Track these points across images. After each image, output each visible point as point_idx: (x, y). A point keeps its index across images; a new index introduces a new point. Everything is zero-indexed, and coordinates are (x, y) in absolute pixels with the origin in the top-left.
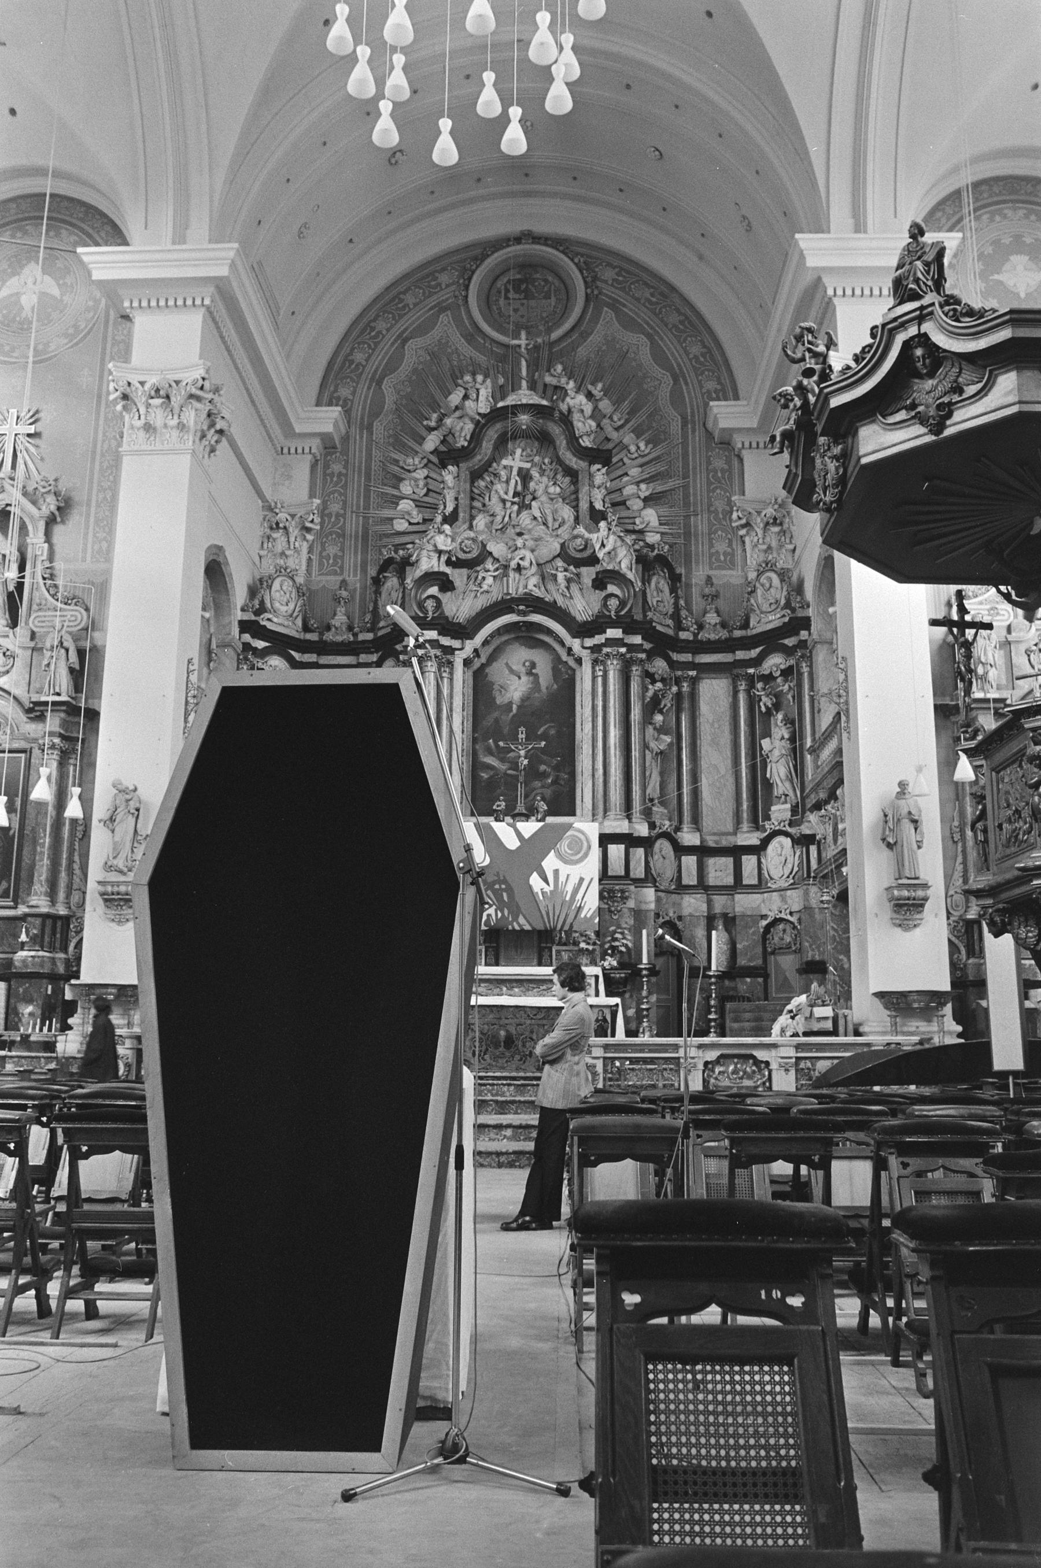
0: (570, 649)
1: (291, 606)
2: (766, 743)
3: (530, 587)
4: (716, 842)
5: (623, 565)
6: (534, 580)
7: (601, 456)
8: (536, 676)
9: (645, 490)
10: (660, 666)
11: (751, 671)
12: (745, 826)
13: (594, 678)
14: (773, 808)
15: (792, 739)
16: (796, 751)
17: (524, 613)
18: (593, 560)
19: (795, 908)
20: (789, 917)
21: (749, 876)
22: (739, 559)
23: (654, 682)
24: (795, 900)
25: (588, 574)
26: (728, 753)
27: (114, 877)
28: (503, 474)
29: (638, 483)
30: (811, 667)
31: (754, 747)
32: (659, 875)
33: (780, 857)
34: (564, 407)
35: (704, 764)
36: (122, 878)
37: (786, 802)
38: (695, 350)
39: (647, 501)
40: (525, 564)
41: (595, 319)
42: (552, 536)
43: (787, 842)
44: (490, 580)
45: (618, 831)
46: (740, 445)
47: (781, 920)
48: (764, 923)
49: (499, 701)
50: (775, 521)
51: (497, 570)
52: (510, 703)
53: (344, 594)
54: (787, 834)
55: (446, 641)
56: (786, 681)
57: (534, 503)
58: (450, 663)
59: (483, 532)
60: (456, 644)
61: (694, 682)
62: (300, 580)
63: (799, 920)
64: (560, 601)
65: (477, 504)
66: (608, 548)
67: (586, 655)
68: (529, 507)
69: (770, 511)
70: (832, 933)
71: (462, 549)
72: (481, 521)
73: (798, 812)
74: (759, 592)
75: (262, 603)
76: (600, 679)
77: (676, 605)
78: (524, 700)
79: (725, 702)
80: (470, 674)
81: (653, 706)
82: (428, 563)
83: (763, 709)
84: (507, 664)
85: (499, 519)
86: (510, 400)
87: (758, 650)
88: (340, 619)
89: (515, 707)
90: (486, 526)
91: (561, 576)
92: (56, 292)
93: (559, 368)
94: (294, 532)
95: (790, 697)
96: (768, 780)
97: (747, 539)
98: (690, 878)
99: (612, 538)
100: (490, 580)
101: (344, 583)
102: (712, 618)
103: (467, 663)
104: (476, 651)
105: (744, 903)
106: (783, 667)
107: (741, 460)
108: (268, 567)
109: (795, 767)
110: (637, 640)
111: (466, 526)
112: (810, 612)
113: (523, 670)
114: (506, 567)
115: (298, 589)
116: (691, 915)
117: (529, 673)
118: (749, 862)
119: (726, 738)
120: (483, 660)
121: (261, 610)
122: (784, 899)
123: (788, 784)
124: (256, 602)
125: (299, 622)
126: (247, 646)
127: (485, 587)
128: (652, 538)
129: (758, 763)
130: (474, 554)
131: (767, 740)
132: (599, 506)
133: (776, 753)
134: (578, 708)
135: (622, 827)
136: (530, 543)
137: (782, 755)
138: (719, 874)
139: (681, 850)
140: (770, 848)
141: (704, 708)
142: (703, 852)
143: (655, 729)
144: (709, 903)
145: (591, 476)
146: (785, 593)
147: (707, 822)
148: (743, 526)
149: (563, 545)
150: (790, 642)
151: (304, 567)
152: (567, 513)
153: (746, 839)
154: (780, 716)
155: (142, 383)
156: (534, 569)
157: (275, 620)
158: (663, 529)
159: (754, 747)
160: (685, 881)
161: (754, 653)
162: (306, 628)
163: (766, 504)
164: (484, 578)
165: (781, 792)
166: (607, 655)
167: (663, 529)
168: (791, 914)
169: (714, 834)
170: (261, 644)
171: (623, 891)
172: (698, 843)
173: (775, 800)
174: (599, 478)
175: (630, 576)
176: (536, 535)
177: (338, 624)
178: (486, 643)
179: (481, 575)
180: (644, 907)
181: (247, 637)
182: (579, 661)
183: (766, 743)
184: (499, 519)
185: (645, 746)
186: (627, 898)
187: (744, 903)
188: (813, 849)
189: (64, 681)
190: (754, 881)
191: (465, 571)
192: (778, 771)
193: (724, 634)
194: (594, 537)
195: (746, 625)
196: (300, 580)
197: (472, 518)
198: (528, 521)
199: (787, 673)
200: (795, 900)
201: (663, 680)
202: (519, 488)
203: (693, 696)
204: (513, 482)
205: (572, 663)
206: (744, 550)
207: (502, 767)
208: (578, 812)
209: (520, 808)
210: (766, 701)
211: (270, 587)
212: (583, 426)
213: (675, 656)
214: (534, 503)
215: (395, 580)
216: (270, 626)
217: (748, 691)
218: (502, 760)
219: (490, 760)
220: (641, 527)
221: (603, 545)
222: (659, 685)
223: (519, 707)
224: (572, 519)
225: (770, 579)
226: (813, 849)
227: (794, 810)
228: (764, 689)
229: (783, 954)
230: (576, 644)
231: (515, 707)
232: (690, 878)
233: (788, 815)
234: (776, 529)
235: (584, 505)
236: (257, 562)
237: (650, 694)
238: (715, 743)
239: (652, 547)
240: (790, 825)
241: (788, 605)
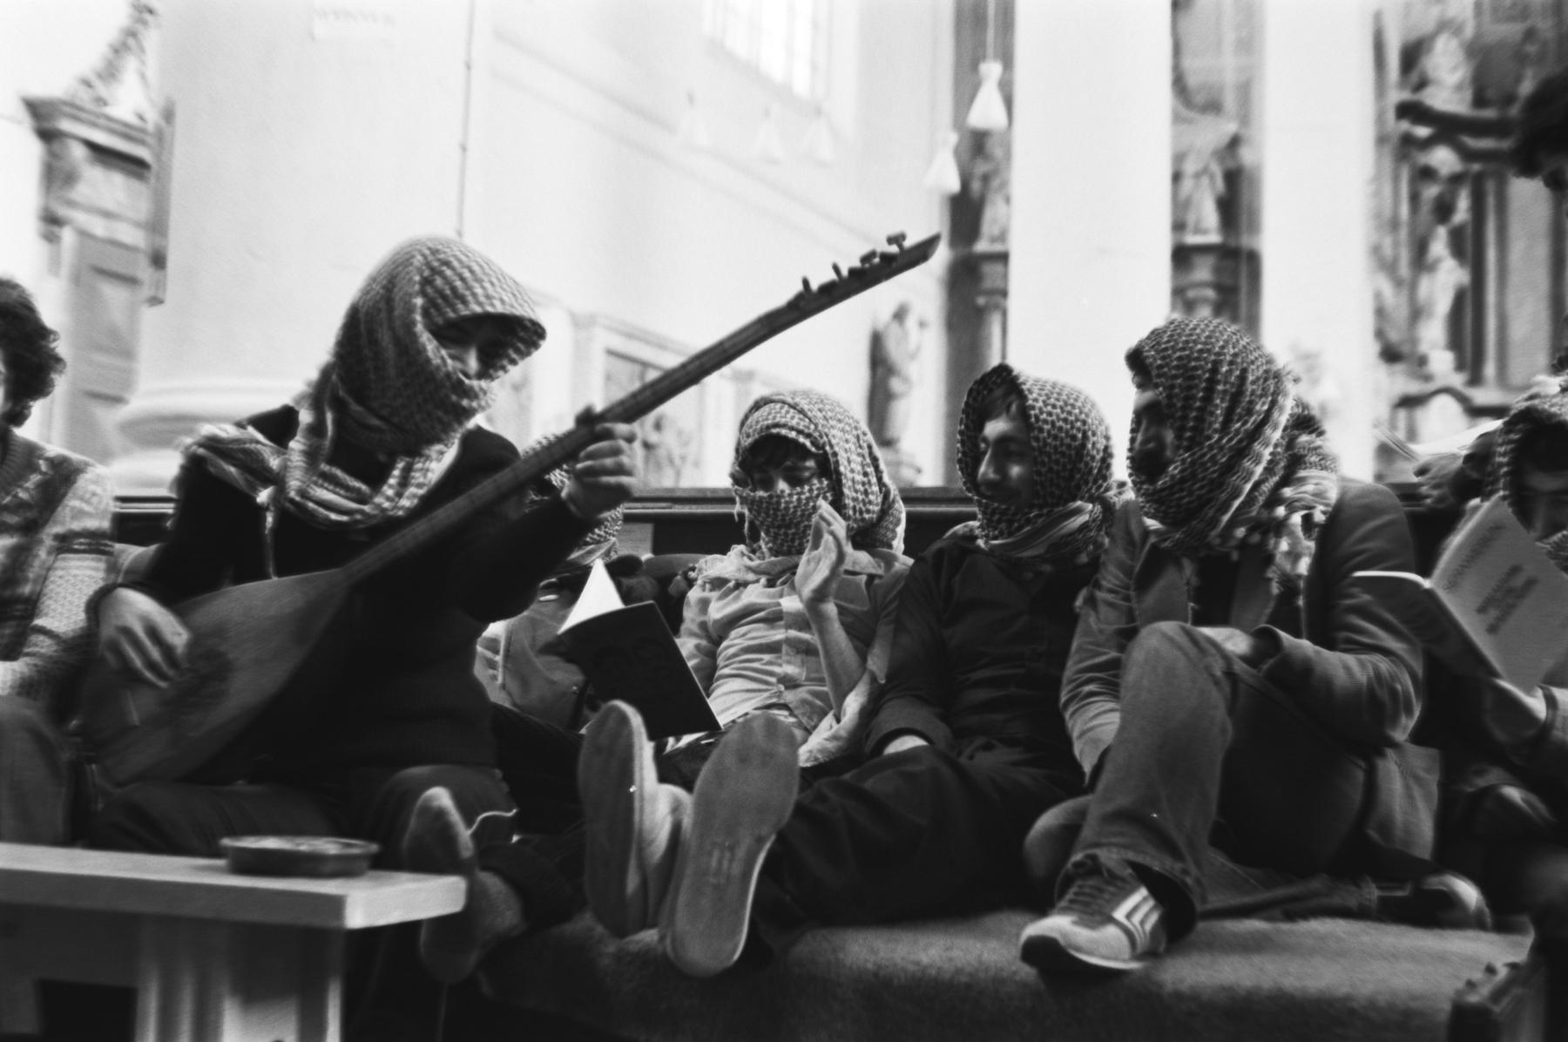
62: (1469, 32)
108: (1426, 20)
121: (1422, 84)
125: (1468, 95)
126: (1408, 141)
162: (1479, 101)
170: (1423, 132)
181: (1405, 126)
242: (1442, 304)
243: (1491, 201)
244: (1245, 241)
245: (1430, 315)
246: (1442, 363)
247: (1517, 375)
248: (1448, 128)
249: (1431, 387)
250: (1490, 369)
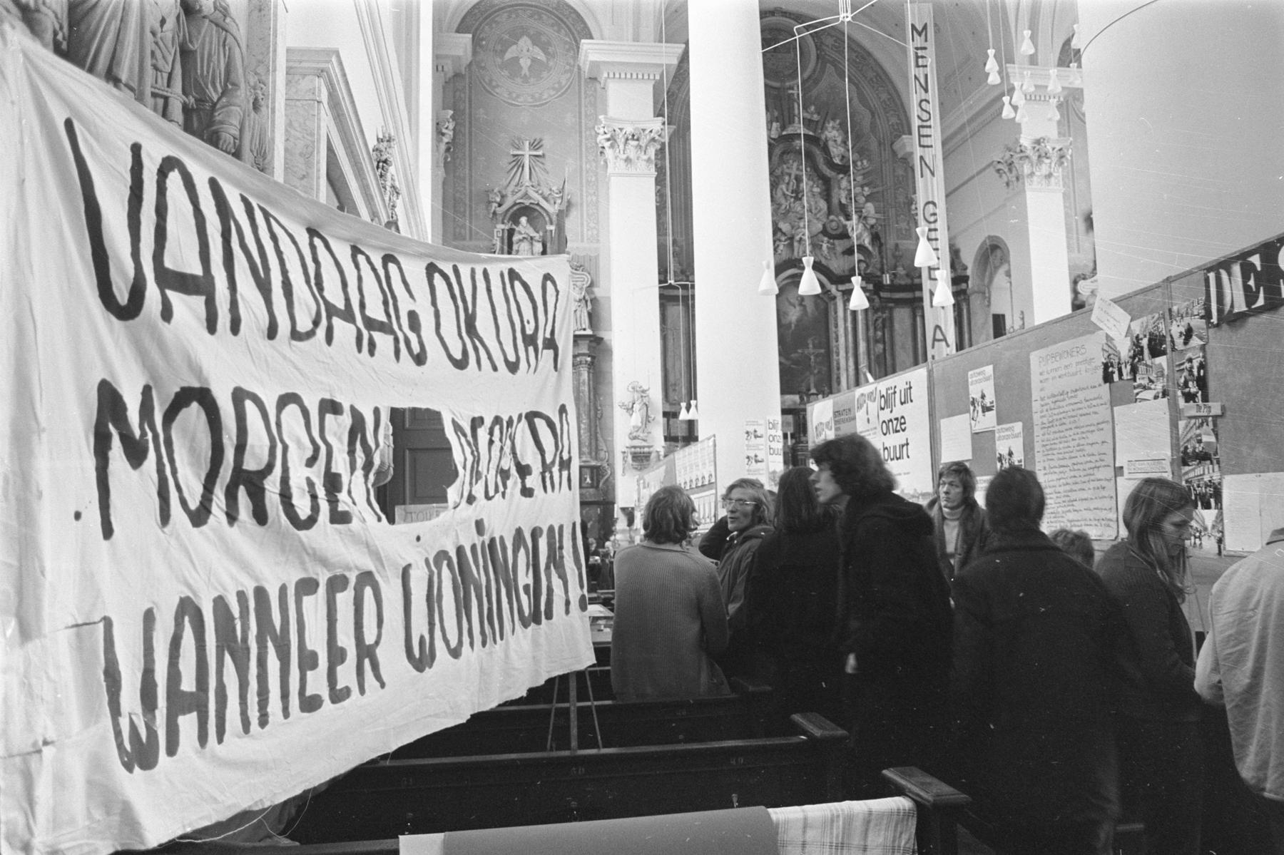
7: (844, 169)
8: (805, 306)
9: (867, 191)
18: (845, 235)
25: (840, 245)
26: (911, 354)
27: (636, 443)
28: (787, 178)
29: (862, 186)
30: (968, 305)
34: (823, 137)
36: (644, 444)
38: (884, 96)
39: (868, 198)
41: (823, 71)
61: (891, 309)
67: (839, 295)
78: (799, 321)
79: (908, 322)
86: (790, 130)
91: (825, 246)
92: (541, 56)
93: (813, 108)
112: (969, 272)
113: (797, 303)
114: (792, 238)
117: (801, 305)
132: (844, 201)
141: (897, 326)
145: (839, 181)
149: (824, 226)
152: (823, 205)
155: (621, 129)
158: (878, 216)
167: (878, 216)
174: (844, 184)
175: (870, 248)
189: (586, 323)
193: (908, 281)
194: (848, 223)
203: (891, 319)
212: (836, 151)
213: (882, 294)
230: (833, 289)
235: (835, 201)
238: (903, 347)
239: (872, 226)
244: (602, 334)
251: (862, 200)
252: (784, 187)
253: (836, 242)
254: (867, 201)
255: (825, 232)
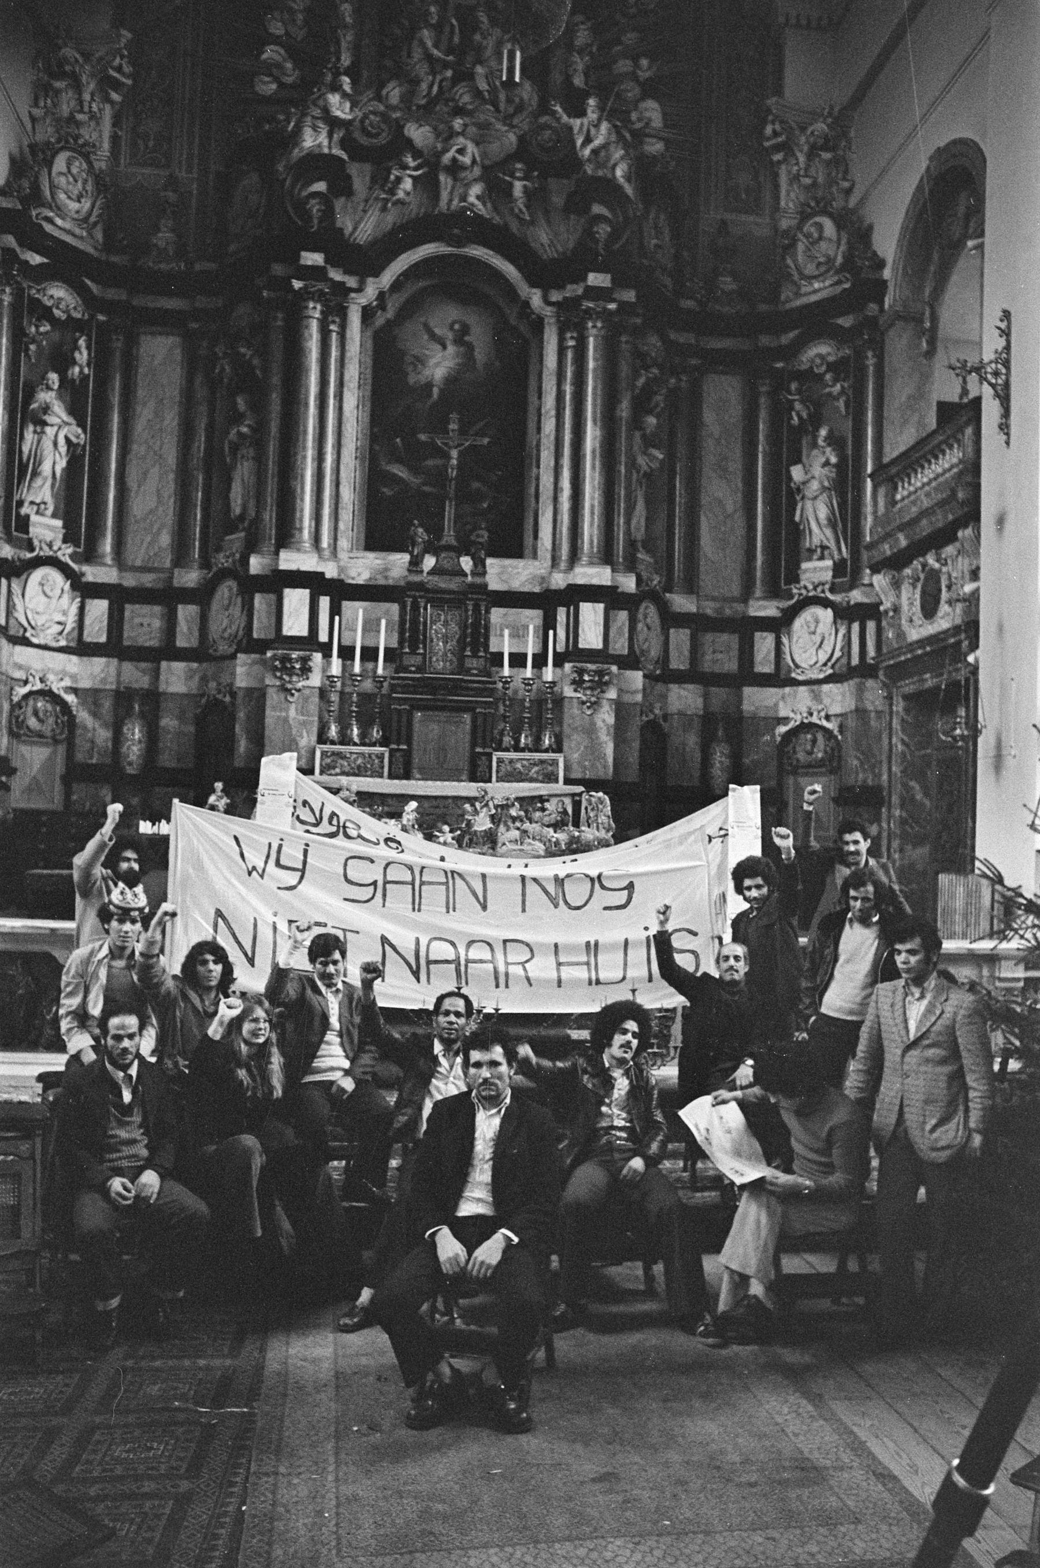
0: (527, 304)
1: (86, 204)
2: (797, 473)
3: (472, 199)
4: (716, 610)
5: (619, 173)
6: (476, 190)
8: (470, 347)
10: (653, 343)
11: (779, 365)
12: (758, 593)
13: (561, 351)
14: (805, 565)
15: (840, 467)
16: (845, 485)
17: (459, 244)
18: (568, 162)
19: (836, 709)
20: (825, 723)
21: (763, 661)
22: (767, 196)
23: (647, 368)
24: (838, 699)
30: (880, 358)
31: (778, 477)
32: (642, 651)
33: (814, 640)
35: (705, 500)
37: (822, 558)
39: (649, 90)
40: (467, 160)
42: (505, 125)
43: (826, 615)
44: (407, 184)
45: (595, 581)
46: (781, 20)
47: (812, 725)
48: (783, 729)
49: (412, 380)
50: (827, 144)
51: (416, 169)
52: (429, 385)
53: (172, 197)
54: (825, 603)
55: (336, 275)
56: (836, 380)
57: (479, 70)
58: (342, 313)
59: (394, 108)
60: (352, 282)
62: (101, 165)
63: (841, 728)
64: (514, 226)
65: (388, 63)
66: (597, 142)
67: (548, 311)
68: (471, 76)
69: (820, 127)
70: (900, 747)
71: (364, 130)
72: (394, 93)
73: (847, 573)
74: (800, 247)
75: (36, 188)
76: (570, 355)
77: (677, 257)
78: (451, 380)
79: (735, 411)
80: (369, 333)
81: (641, 406)
82: (314, 139)
83: (796, 420)
84: (426, 325)
85: (424, 86)
87: (792, 335)
88: (164, 237)
89: (436, 391)
90: (403, 98)
91: (518, 187)
94: (91, 86)
95: (841, 404)
96: (797, 525)
97: (783, 171)
98: (678, 662)
99: (604, 126)
100: (407, 184)
101: (172, 182)
102: (727, 283)
103: (367, 314)
104: (381, 296)
105: (757, 699)
106: (831, 359)
107: (779, 48)
108: (46, 133)
109: (842, 505)
110: (630, 296)
111: (370, 94)
113: (450, 335)
115: (97, 176)
116: (680, 713)
117: (459, 341)
118: (764, 643)
119: (736, 465)
120: (390, 314)
122: (817, 697)
123: (829, 532)
124: (26, 184)
125: (99, 236)
127: (401, 194)
128: (655, 147)
129: (785, 498)
130: (383, 139)
131: (799, 467)
132: (578, 81)
133: (815, 485)
134: (533, 399)
135: (601, 576)
136: (472, 130)
137: (824, 489)
138: (720, 656)
139: (670, 619)
140: (798, 623)
141: (708, 416)
142: (698, 624)
143: (644, 437)
144: (706, 696)
146: (843, 248)
147: (706, 580)
148: (777, 148)
149: (521, 139)
150: (846, 322)
151: (106, 145)
153: (760, 608)
154: (823, 432)
156: (477, 171)
157: (59, 222)
159: (778, 477)
160: (674, 665)
161: (787, 338)
162: (109, 245)
163: (815, 115)
164: (399, 180)
165: (816, 541)
166: (588, 311)
168: (828, 718)
169: (714, 599)
170: (36, 259)
171: (601, 673)
172: (693, 609)
173: (804, 554)
176: (482, 117)
177: (162, 244)
178: (396, 286)
179: (395, 173)
180: (627, 698)
182: (538, 326)
183: (797, 473)
184: (424, 86)
185: (632, 464)
186: (607, 684)
187: (757, 699)
188: (871, 626)
190: (768, 669)
191: (367, 167)
192: (816, 514)
194: (576, 123)
195: (774, 296)
196: (101, 165)
197: (382, 85)
198: (466, 98)
199: (838, 368)
200: (838, 699)
201: (661, 367)
202: (456, 40)
204: (447, 29)
205: (523, 328)
206: (777, 187)
207: (415, 481)
208: (527, 551)
209: (449, 537)
210: (799, 411)
211: (50, 164)
214: (479, 70)
215: (255, 177)
216: (48, 228)
217: (773, 394)
218: (415, 470)
219: (400, 471)
220: (638, 126)
221: (588, 140)
222: (655, 371)
223: (442, 391)
224: (534, 103)
225: (820, 227)
226: (871, 626)
227: (839, 569)
228: (799, 391)
229: (806, 774)
231: (436, 391)
232: (678, 662)
233: (828, 576)
234: (827, 156)
236: (29, 127)
237: (641, 382)
240: (832, 590)
241: (849, 265)
242: (54, 462)
243: (117, 359)
245: (35, 474)
246: (46, 530)
247: (136, 555)
248: (65, 263)
249: (29, 555)
250: (107, 546)
251: (631, 91)
252: (427, 35)
253: (553, 183)
254: (643, 99)
255: (523, 151)
